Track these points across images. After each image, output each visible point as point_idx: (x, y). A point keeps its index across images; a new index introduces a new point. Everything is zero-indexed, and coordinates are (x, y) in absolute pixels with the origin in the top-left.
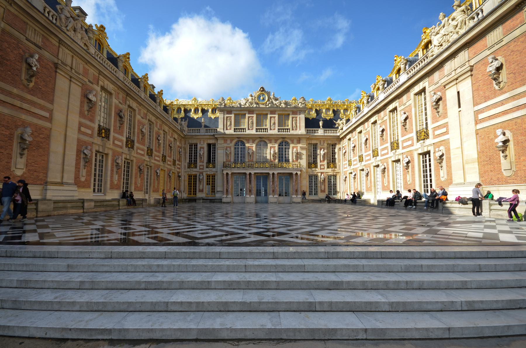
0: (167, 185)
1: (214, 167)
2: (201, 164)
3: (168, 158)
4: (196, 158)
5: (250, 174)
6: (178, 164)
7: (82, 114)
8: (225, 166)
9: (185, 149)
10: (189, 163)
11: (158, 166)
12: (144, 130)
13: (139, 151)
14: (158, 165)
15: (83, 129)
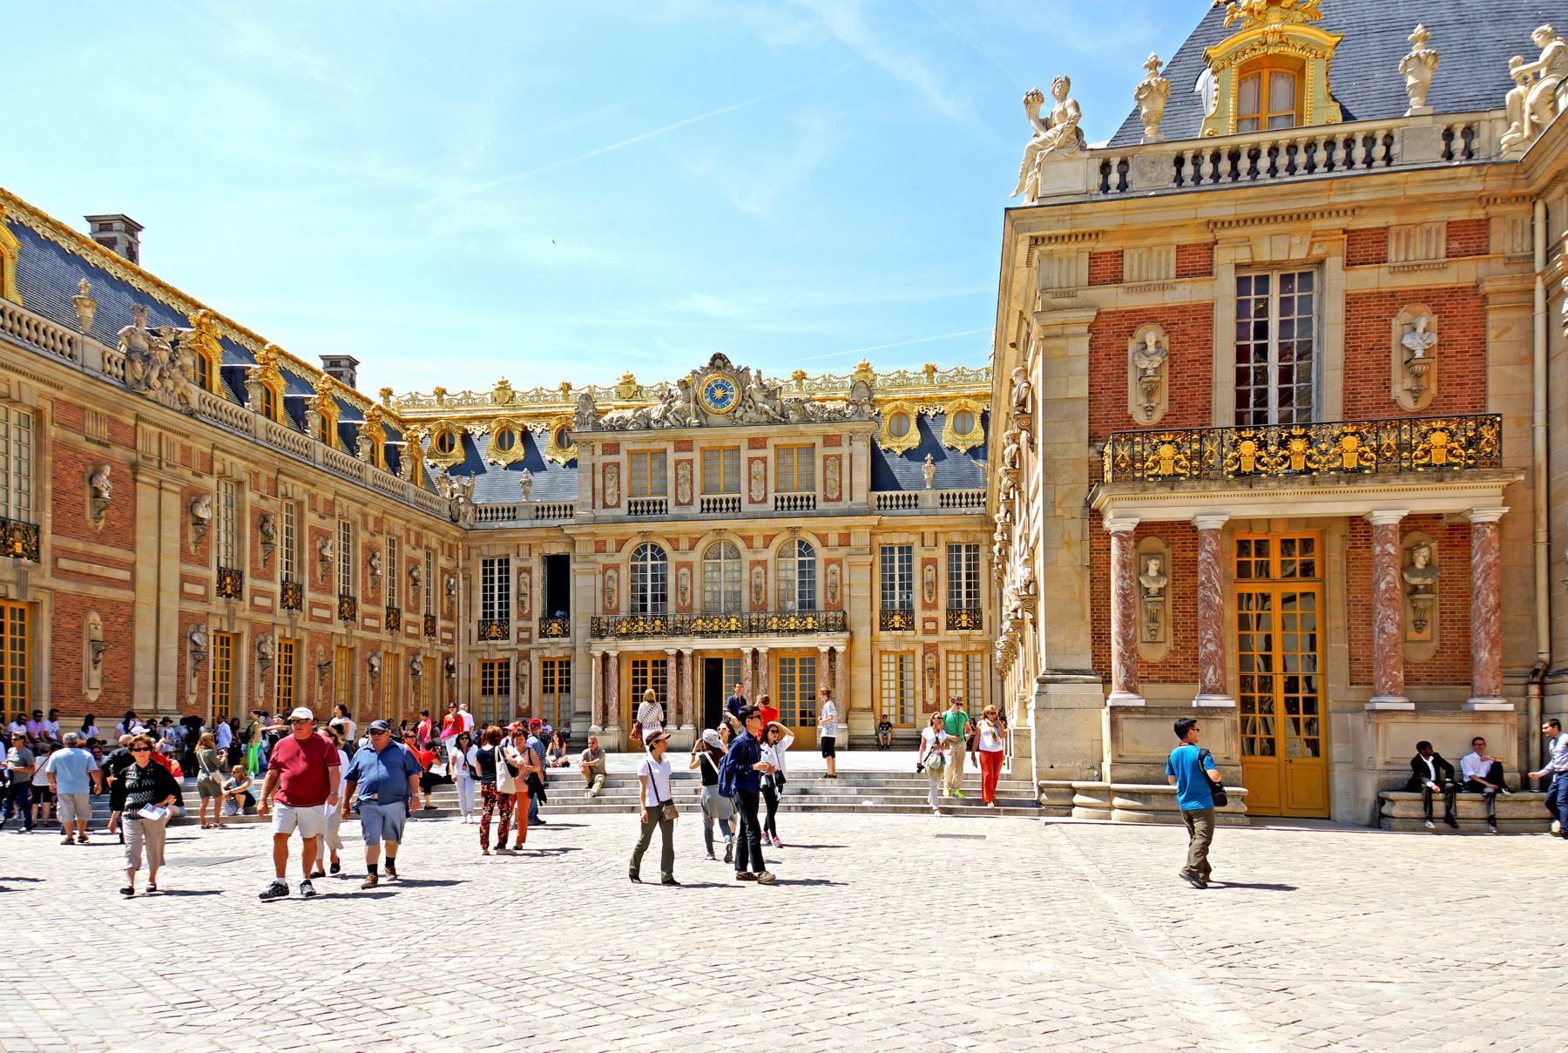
0: (406, 701)
1: (565, 633)
2: (523, 624)
3: (406, 616)
4: (507, 605)
5: (679, 655)
6: (444, 629)
7: (185, 556)
8: (598, 632)
9: (468, 578)
10: (484, 622)
11: (374, 647)
12: (327, 552)
13: (316, 612)
14: (373, 642)
15: (188, 587)
